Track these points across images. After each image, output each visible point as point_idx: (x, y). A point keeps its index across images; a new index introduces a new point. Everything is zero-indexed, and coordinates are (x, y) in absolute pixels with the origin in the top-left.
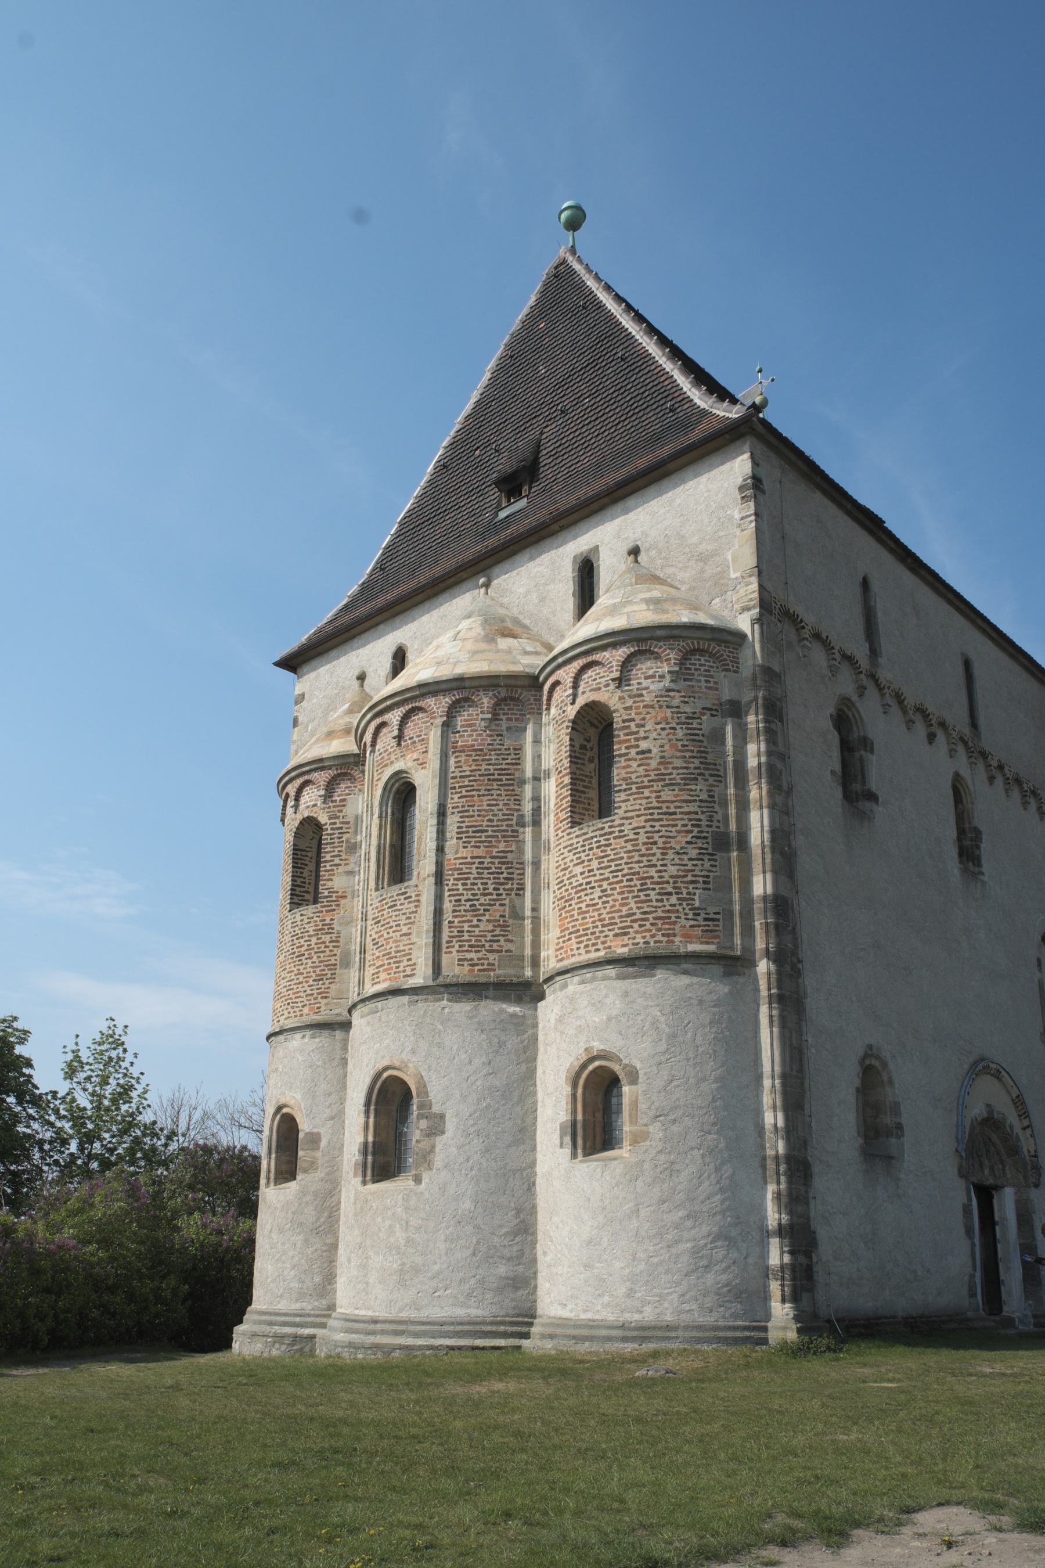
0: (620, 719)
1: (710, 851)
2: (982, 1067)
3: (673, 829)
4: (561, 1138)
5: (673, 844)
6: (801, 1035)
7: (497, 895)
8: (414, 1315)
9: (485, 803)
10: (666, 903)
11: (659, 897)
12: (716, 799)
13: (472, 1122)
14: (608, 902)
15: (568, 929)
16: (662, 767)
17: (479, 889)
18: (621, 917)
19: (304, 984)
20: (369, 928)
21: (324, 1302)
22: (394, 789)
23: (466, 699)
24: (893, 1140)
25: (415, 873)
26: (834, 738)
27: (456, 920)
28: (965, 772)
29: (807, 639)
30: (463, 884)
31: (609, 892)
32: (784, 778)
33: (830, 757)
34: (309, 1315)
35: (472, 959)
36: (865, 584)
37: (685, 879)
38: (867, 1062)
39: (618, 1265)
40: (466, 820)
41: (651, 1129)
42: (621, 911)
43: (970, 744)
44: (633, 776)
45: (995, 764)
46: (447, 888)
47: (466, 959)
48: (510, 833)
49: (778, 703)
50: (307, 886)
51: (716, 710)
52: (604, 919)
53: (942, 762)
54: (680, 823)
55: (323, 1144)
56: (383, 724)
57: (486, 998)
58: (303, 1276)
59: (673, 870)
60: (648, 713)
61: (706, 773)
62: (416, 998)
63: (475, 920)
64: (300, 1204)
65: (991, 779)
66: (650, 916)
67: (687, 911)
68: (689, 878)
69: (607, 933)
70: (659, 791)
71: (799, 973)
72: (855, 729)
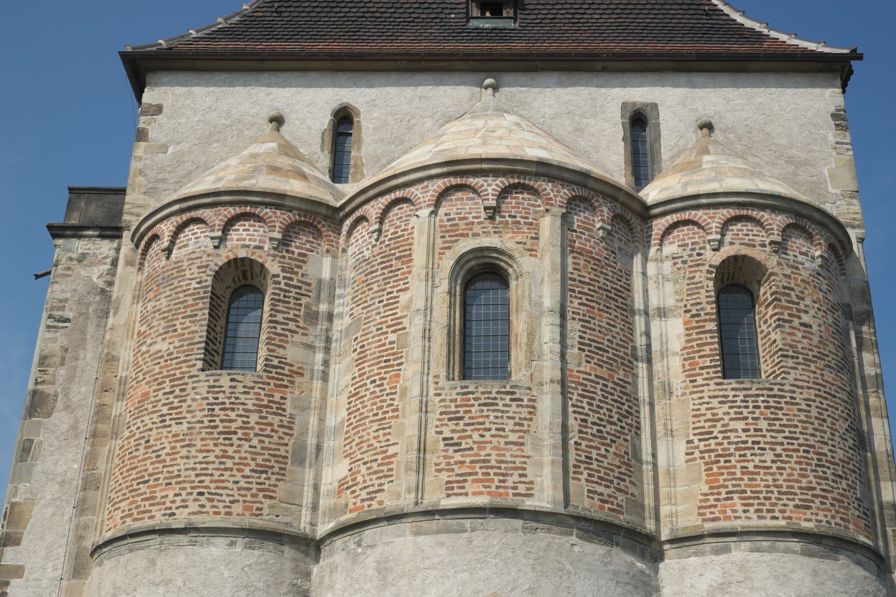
9: (605, 320)
14: (784, 469)
17: (604, 414)
22: (468, 266)
23: (583, 199)
46: (570, 403)
47: (595, 492)
57: (617, 545)
62: (535, 525)
63: (603, 448)
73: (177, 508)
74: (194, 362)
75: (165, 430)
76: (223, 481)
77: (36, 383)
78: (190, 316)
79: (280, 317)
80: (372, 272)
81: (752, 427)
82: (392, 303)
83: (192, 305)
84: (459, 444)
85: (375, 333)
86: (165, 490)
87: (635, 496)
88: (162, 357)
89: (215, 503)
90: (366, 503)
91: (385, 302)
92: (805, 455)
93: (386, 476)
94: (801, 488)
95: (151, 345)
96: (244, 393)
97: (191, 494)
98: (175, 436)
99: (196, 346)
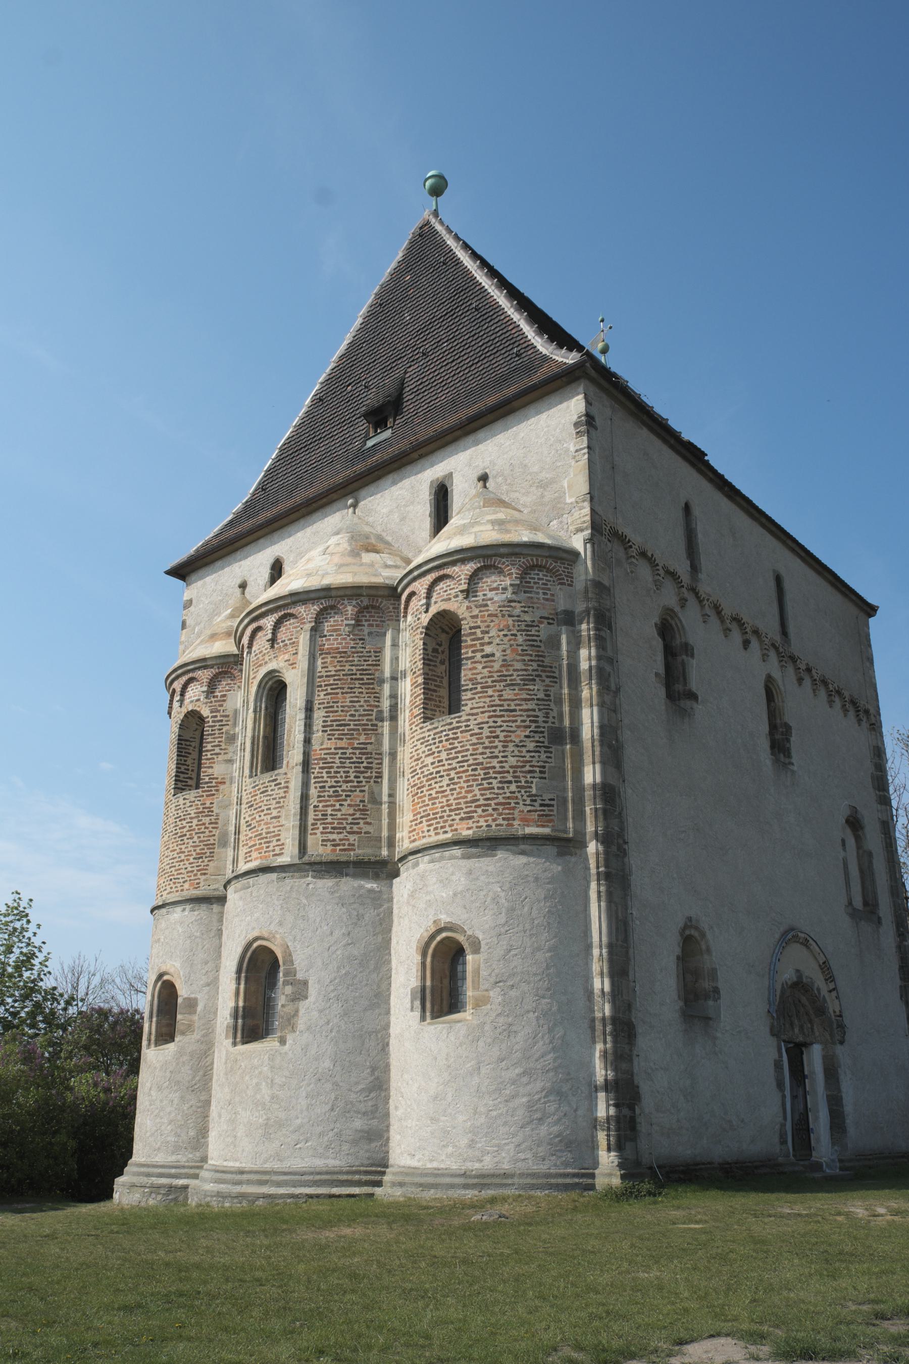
0: (467, 626)
1: (546, 744)
2: (792, 937)
3: (513, 725)
4: (412, 1002)
5: (513, 738)
6: (626, 909)
7: (358, 782)
8: (277, 1166)
9: (348, 700)
10: (506, 790)
11: (500, 785)
12: (552, 698)
13: (332, 988)
14: (455, 789)
15: (419, 813)
16: (503, 669)
17: (341, 777)
18: (466, 802)
19: (186, 862)
20: (243, 811)
21: (198, 1154)
22: (268, 686)
23: (333, 607)
24: (711, 1003)
25: (285, 762)
26: (658, 643)
27: (321, 805)
28: (777, 675)
29: (634, 557)
30: (327, 773)
31: (456, 780)
32: (612, 679)
33: (655, 661)
34: (184, 1167)
35: (334, 840)
36: (687, 508)
37: (523, 769)
38: (687, 932)
39: (461, 1118)
40: (331, 714)
41: (491, 993)
42: (466, 797)
43: (781, 650)
44: (479, 677)
45: (803, 667)
46: (313, 776)
47: (329, 840)
48: (370, 727)
49: (607, 614)
50: (190, 772)
51: (553, 619)
52: (452, 805)
53: (757, 666)
54: (519, 719)
55: (200, 1008)
56: (259, 629)
57: (347, 875)
58: (179, 1131)
59: (512, 761)
60: (492, 621)
61: (544, 674)
62: (284, 875)
63: (337, 804)
64: (178, 1064)
65: (800, 680)
66: (492, 802)
67: (525, 798)
68: (527, 768)
69: (454, 817)
70: (502, 691)
71: (624, 853)
72: (678, 636)
87: (369, 833)
92: (473, 773)
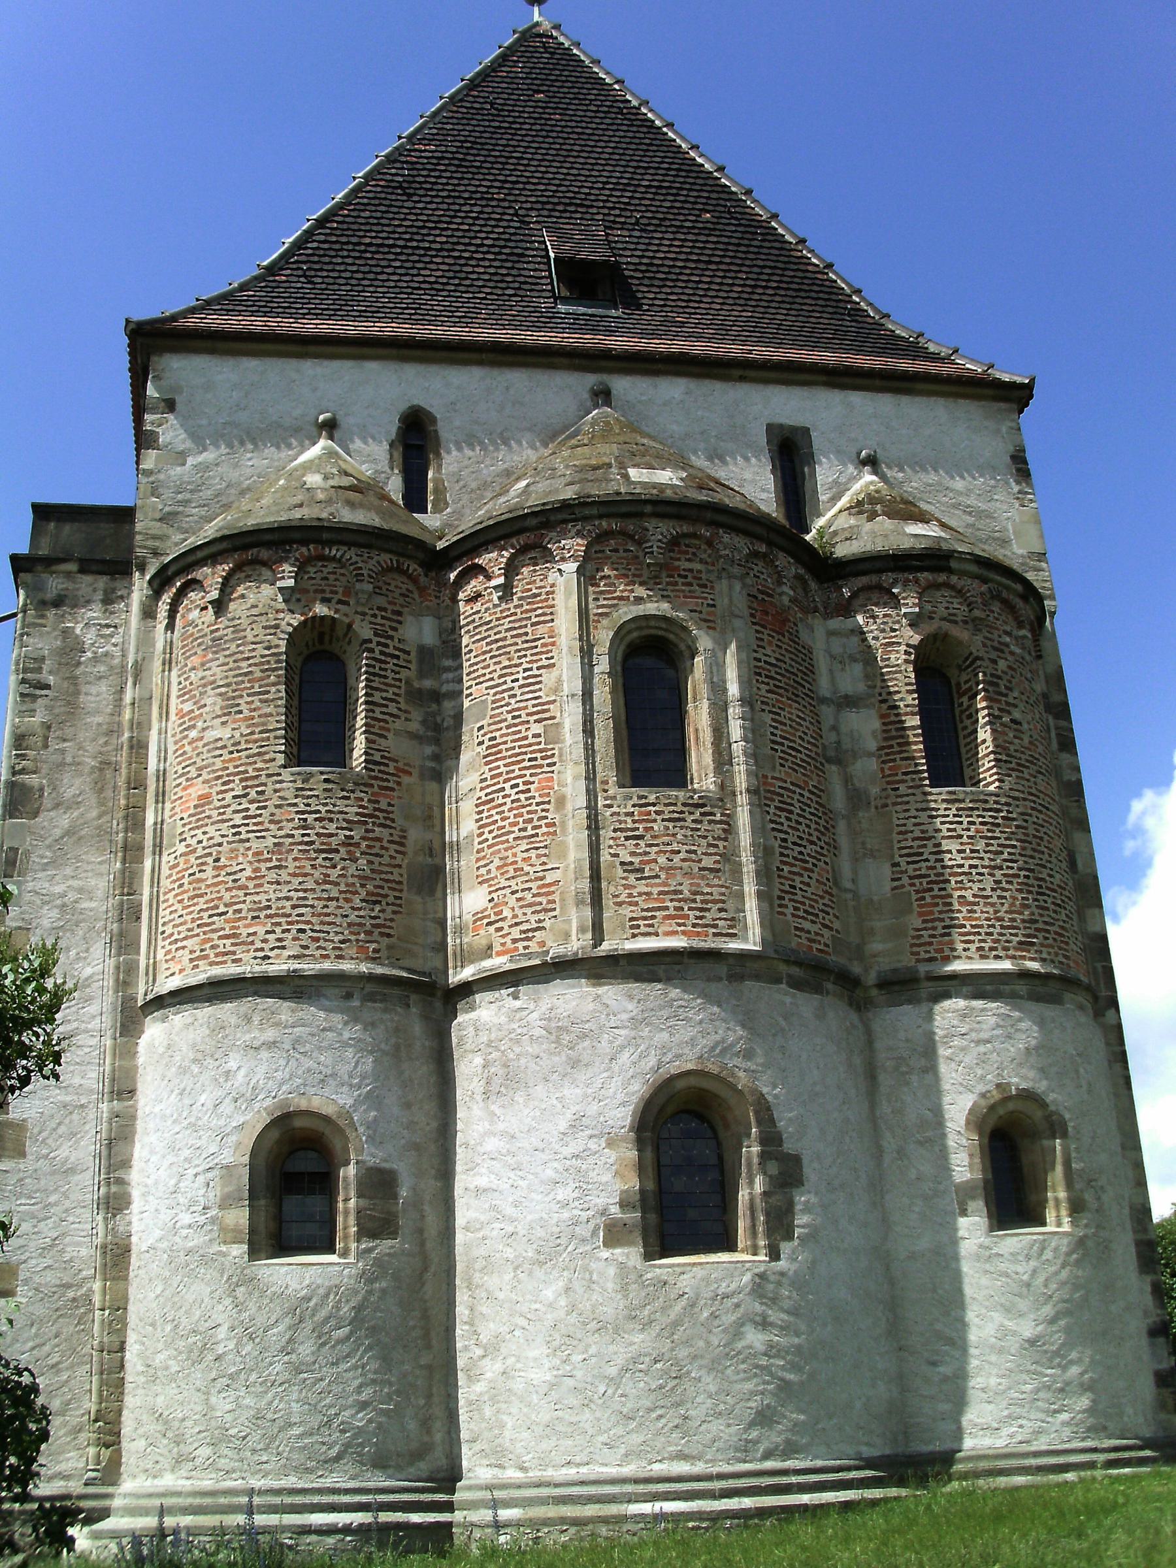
47: (802, 930)
63: (806, 874)
73: (272, 949)
74: (272, 755)
75: (241, 847)
76: (328, 915)
77: (14, 774)
78: (260, 693)
79: (377, 697)
80: (497, 641)
81: (968, 848)
82: (533, 682)
83: (262, 679)
84: (642, 870)
85: (510, 721)
86: (249, 926)
88: (224, 747)
89: (322, 943)
90: (520, 945)
91: (521, 682)
93: (546, 910)
94: (1023, 921)
95: (204, 729)
96: (344, 798)
97: (288, 931)
98: (256, 854)
99: (272, 735)
